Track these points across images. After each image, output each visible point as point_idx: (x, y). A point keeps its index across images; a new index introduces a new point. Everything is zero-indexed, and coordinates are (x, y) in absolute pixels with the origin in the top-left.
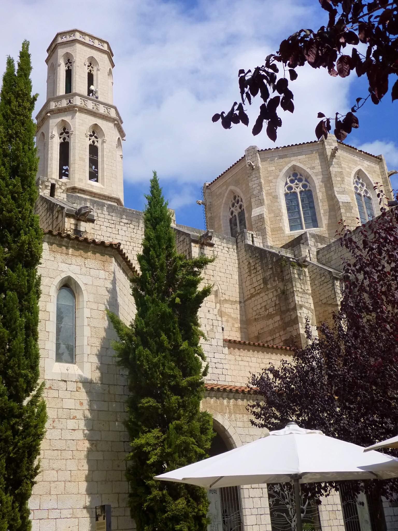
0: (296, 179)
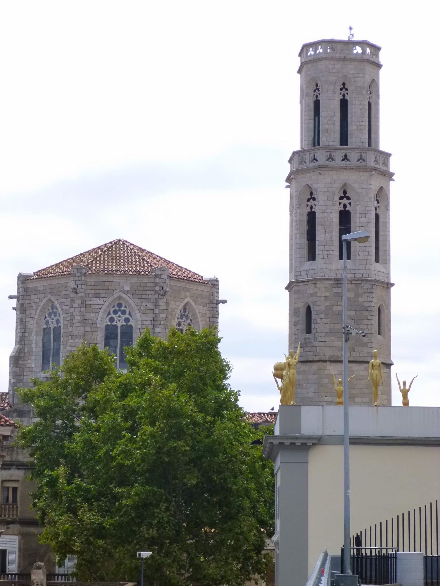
0: (120, 310)
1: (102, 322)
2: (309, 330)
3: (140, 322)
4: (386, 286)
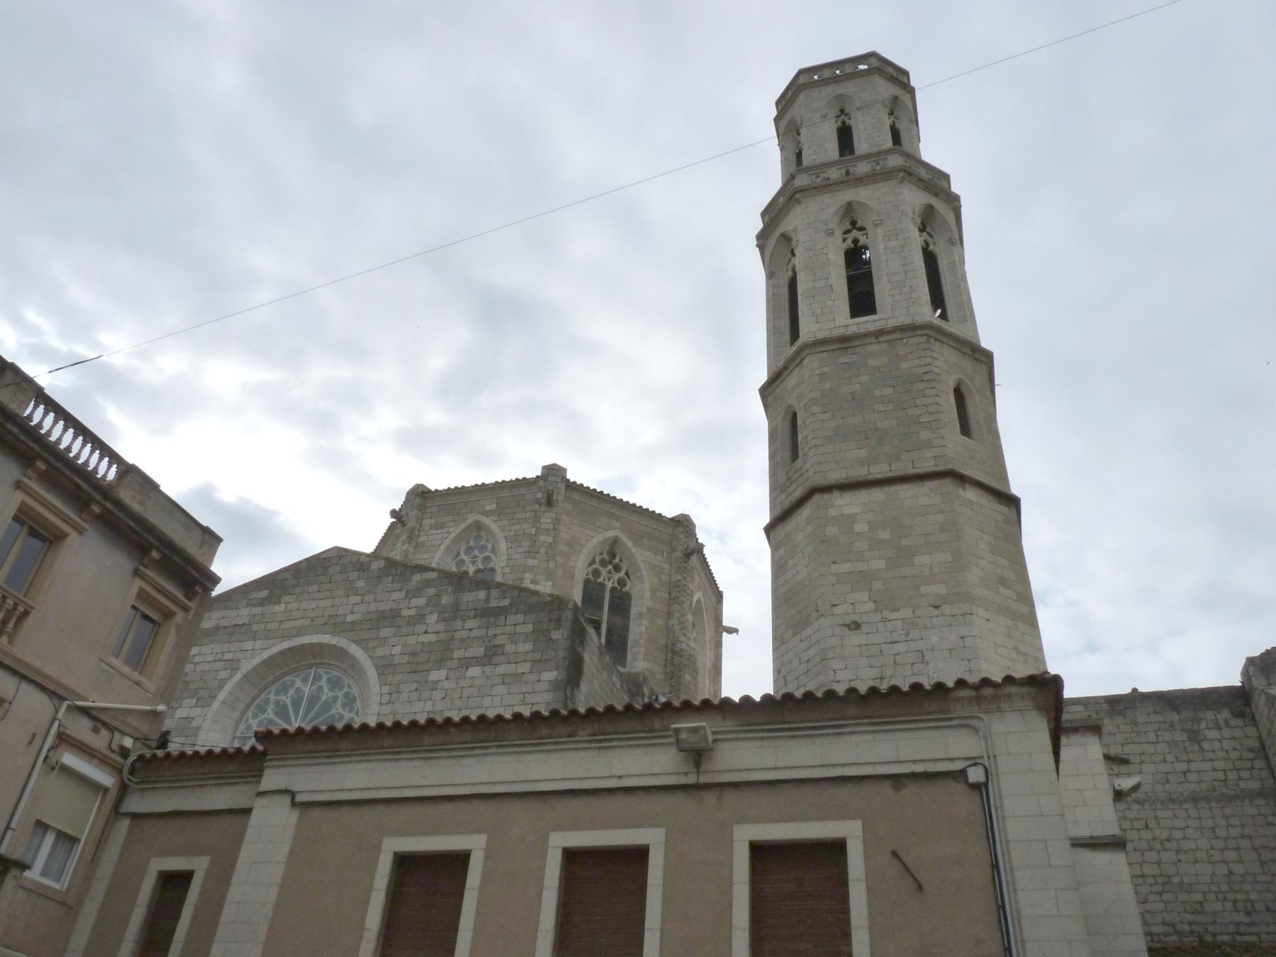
4: (969, 352)
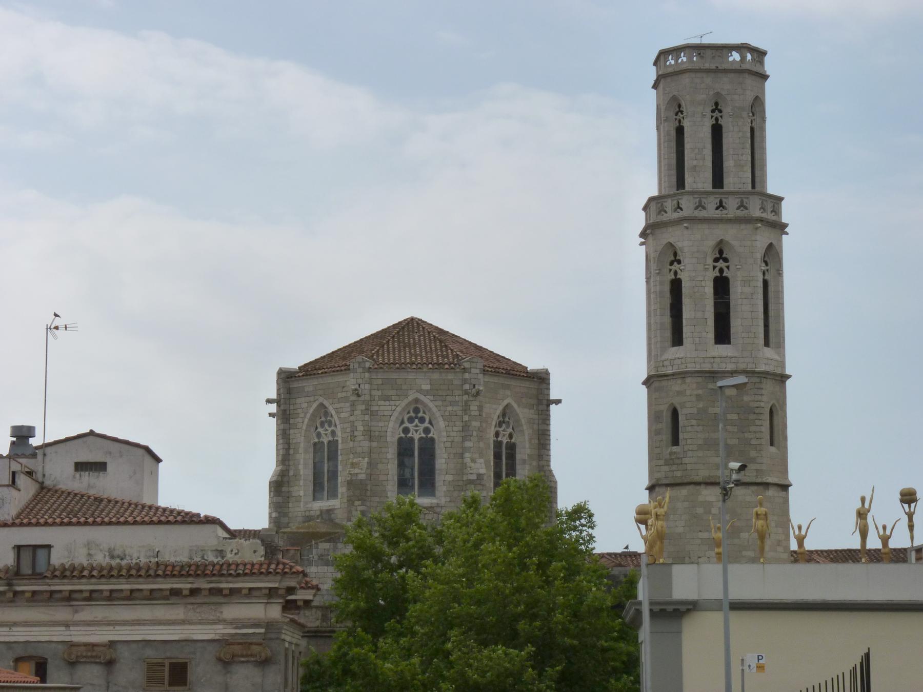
0: (416, 417)
1: (393, 433)
2: (675, 441)
3: (444, 434)
